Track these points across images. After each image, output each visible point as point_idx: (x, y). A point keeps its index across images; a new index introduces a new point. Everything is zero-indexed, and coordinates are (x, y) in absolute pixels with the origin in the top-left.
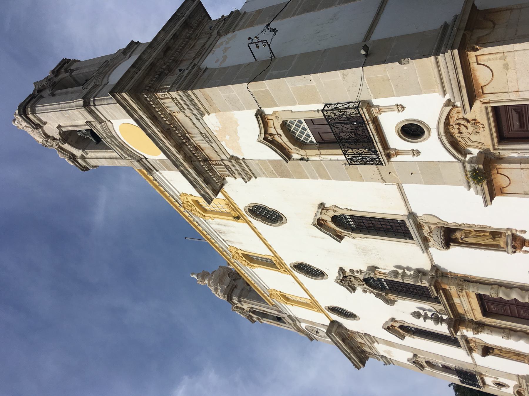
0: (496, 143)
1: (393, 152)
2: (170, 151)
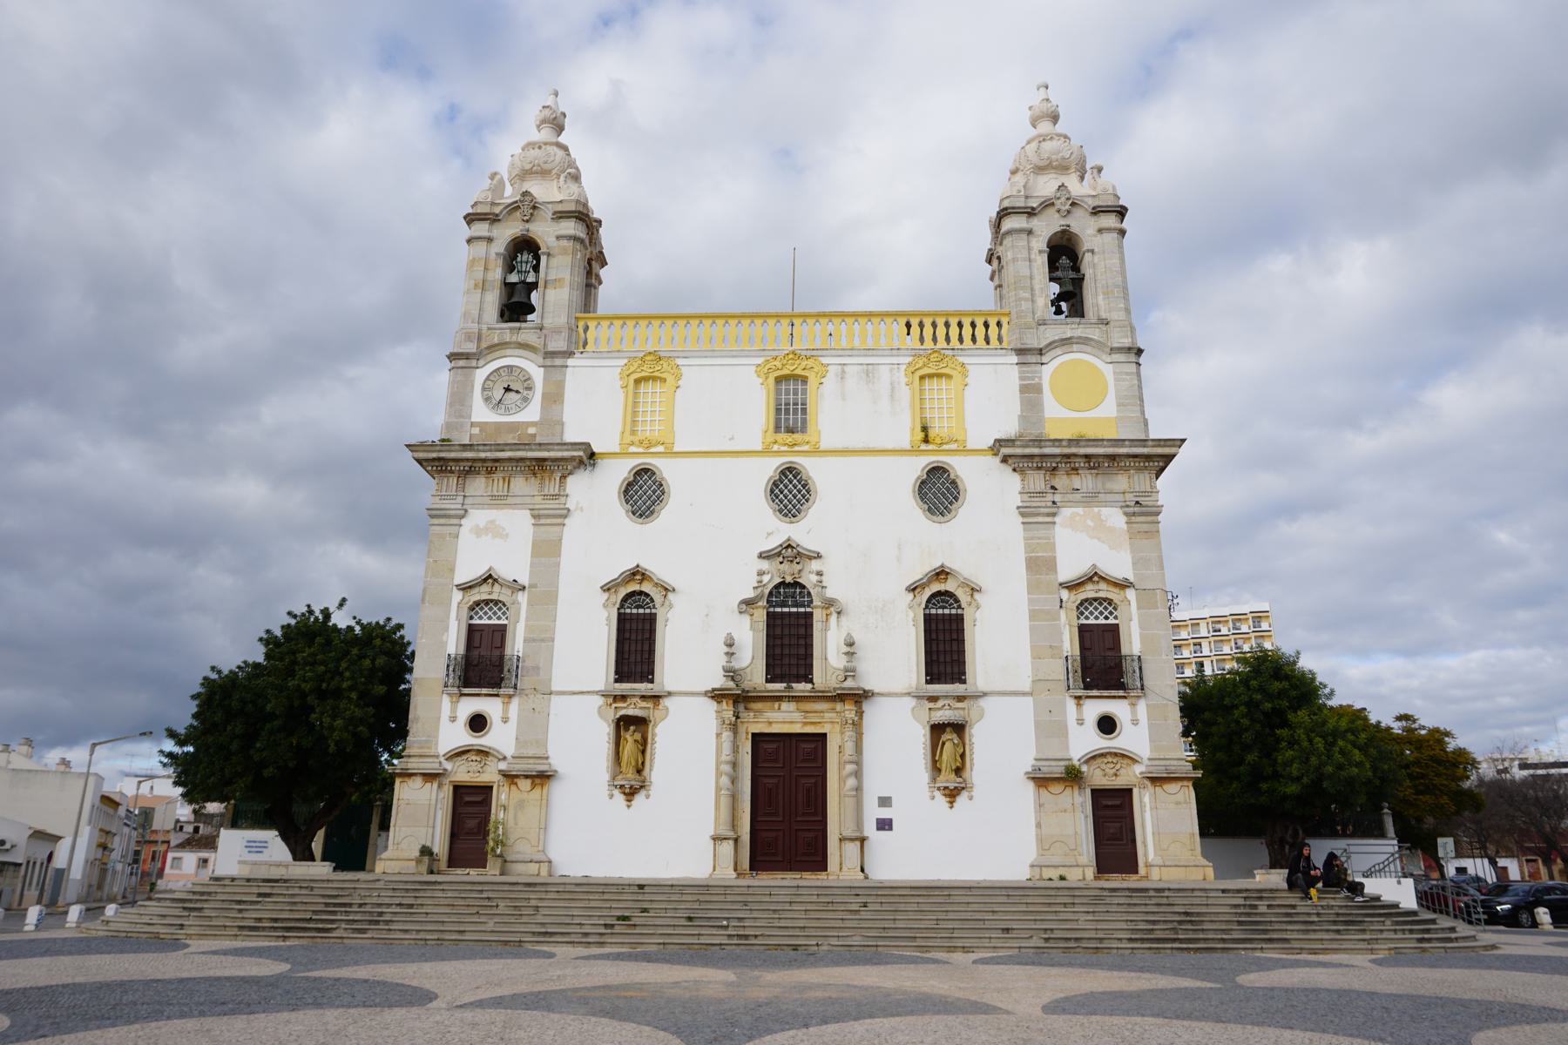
0: (1093, 787)
1: (1081, 702)
2: (1092, 446)
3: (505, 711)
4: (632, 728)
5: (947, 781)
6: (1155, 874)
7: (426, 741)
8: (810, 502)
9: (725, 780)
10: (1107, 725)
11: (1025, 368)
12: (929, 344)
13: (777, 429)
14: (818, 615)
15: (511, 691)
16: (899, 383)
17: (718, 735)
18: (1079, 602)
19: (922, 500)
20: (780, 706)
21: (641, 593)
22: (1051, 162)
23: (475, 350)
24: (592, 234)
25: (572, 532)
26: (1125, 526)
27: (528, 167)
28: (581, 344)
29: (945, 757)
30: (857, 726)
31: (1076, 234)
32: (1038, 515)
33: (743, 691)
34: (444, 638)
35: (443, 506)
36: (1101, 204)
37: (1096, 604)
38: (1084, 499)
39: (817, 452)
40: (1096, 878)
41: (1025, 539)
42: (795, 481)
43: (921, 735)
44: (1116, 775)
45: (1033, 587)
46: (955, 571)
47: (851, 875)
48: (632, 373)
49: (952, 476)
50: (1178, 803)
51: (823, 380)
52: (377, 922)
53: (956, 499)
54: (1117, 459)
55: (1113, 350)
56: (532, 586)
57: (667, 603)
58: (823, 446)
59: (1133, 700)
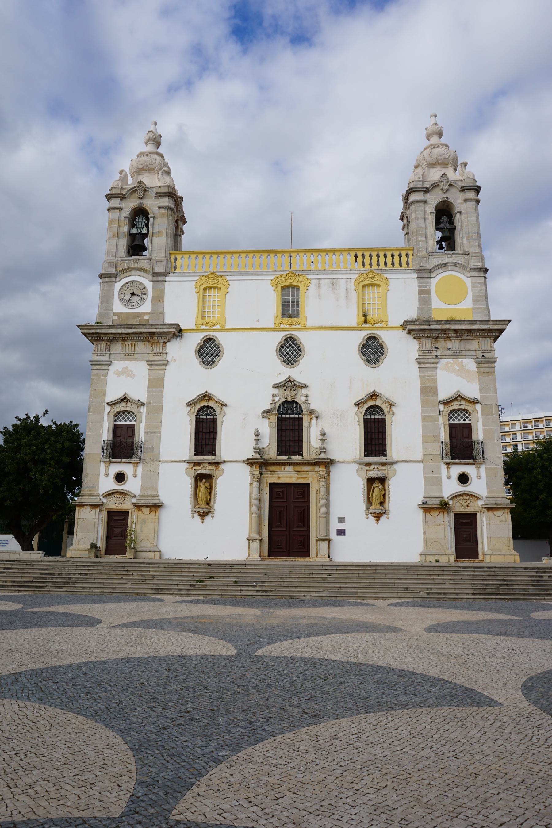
1: (450, 466)
2: (458, 324)
3: (135, 471)
4: (204, 480)
5: (375, 509)
6: (488, 559)
7: (93, 487)
8: (301, 356)
9: (254, 509)
10: (463, 479)
11: (422, 281)
12: (367, 267)
13: (283, 316)
14: (305, 419)
15: (138, 460)
16: (351, 290)
17: (251, 484)
18: (449, 411)
19: (363, 355)
20: (284, 468)
21: (208, 407)
22: (437, 161)
23: (114, 272)
24: (178, 205)
25: (170, 373)
26: (476, 369)
27: (141, 166)
28: (173, 268)
29: (374, 496)
30: (327, 479)
31: (452, 203)
32: (428, 363)
33: (265, 460)
34: (101, 432)
35: (99, 359)
36: (466, 185)
37: (459, 412)
38: (454, 354)
39: (305, 328)
40: (455, 561)
41: (420, 376)
42: (293, 345)
43: (361, 485)
44: (468, 506)
45: (424, 403)
46: (381, 394)
47: (323, 559)
48: (202, 284)
49: (380, 342)
50: (501, 521)
51: (308, 288)
52: (68, 583)
53: (382, 354)
54: (472, 332)
55: (471, 270)
56: (148, 403)
57: (222, 412)
58: (309, 324)
59: (478, 465)
